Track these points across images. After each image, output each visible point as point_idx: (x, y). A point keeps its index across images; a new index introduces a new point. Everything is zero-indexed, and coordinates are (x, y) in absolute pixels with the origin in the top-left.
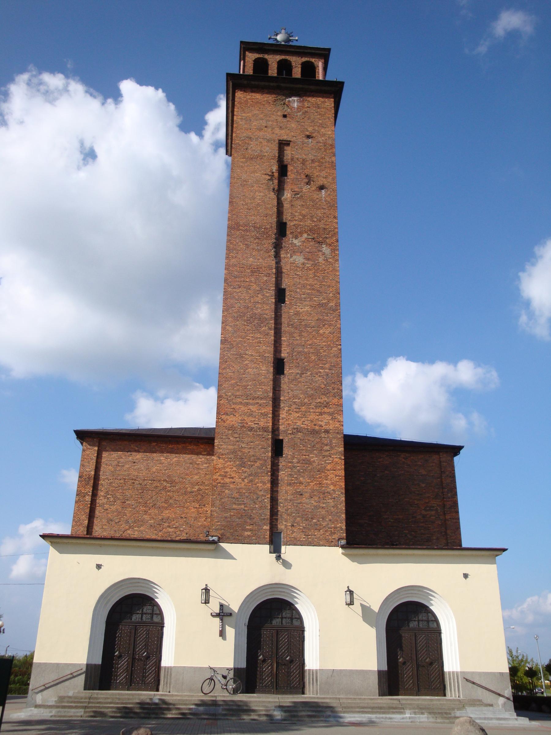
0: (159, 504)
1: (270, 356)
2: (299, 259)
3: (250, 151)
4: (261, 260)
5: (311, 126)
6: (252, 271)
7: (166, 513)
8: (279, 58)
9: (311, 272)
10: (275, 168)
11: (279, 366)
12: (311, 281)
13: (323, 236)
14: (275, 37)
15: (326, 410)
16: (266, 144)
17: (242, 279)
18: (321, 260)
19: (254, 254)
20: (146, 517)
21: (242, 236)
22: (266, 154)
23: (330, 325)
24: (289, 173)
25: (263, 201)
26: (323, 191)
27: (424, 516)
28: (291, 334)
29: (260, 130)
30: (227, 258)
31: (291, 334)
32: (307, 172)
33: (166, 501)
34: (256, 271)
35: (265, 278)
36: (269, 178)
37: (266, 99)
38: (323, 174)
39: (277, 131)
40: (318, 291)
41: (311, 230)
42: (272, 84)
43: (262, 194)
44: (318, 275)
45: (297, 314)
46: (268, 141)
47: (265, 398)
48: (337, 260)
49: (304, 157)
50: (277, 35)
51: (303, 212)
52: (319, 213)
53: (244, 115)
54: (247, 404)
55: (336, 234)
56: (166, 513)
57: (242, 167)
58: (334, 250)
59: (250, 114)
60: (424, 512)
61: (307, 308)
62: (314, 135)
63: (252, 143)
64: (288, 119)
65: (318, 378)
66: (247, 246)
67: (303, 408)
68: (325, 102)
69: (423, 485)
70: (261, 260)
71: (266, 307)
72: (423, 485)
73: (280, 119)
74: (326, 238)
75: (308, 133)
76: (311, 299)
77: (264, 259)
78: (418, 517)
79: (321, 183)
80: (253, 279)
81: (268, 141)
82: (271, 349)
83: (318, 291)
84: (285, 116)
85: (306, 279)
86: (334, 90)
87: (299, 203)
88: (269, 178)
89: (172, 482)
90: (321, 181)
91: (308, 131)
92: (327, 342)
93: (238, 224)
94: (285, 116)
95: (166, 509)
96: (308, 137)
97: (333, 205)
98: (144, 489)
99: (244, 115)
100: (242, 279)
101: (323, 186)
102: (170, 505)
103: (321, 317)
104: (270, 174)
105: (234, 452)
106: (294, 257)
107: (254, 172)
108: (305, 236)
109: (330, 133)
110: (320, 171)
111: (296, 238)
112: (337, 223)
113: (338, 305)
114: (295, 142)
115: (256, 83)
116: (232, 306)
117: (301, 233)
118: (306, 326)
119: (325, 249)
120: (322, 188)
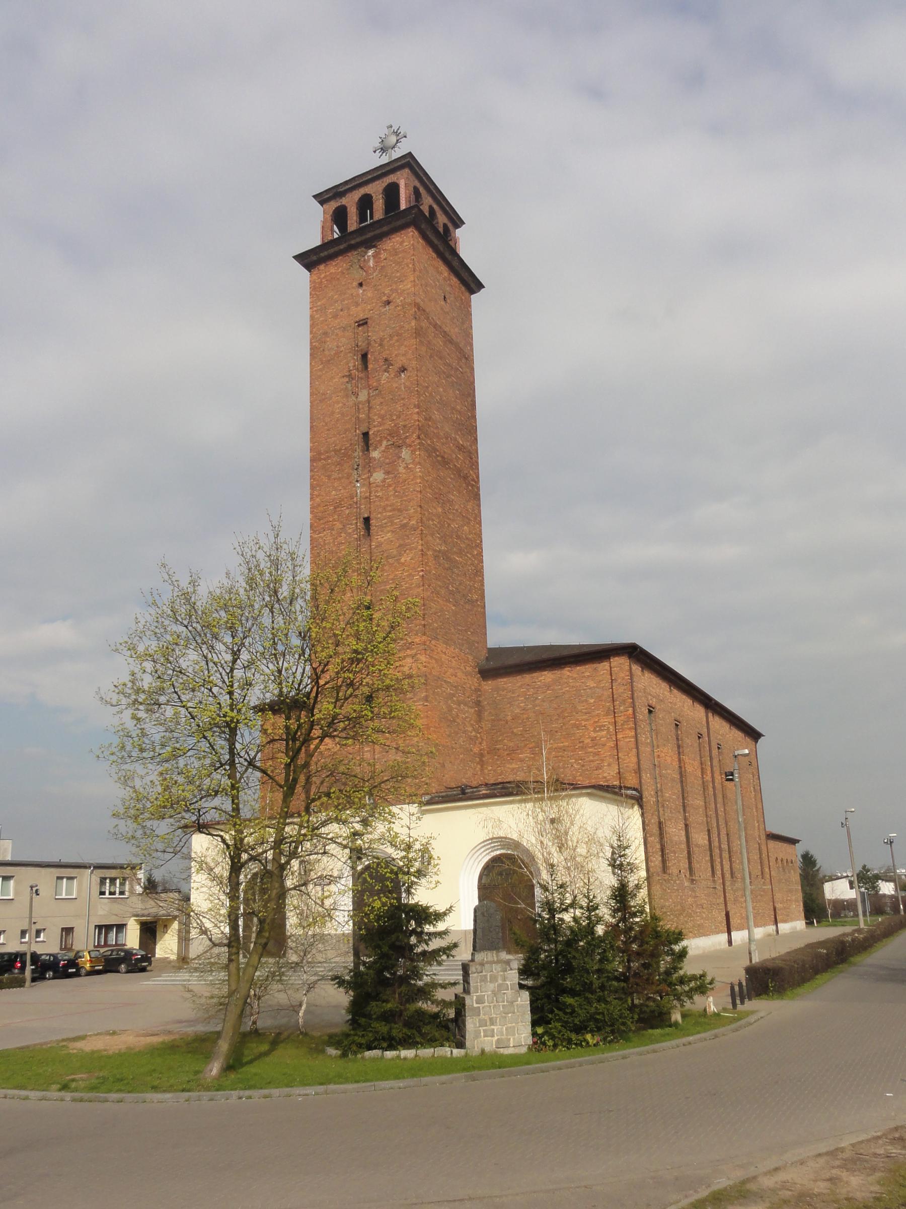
2: (378, 476)
3: (327, 352)
6: (335, 508)
8: (356, 195)
15: (409, 652)
17: (325, 520)
18: (401, 469)
23: (411, 550)
27: (593, 739)
29: (335, 316)
30: (312, 499)
36: (347, 380)
39: (354, 310)
40: (399, 510)
42: (342, 247)
44: (398, 489)
45: (379, 545)
51: (383, 412)
57: (320, 377)
60: (593, 734)
64: (364, 287)
66: (329, 477)
68: (401, 243)
69: (592, 701)
72: (592, 701)
74: (406, 437)
75: (385, 298)
76: (392, 522)
77: (345, 489)
78: (586, 741)
80: (336, 517)
84: (361, 285)
85: (387, 499)
88: (347, 380)
90: (400, 361)
91: (385, 294)
92: (408, 571)
93: (320, 454)
94: (361, 285)
100: (325, 520)
101: (403, 367)
103: (402, 542)
106: (374, 475)
108: (385, 443)
115: (326, 253)
117: (380, 442)
118: (387, 557)
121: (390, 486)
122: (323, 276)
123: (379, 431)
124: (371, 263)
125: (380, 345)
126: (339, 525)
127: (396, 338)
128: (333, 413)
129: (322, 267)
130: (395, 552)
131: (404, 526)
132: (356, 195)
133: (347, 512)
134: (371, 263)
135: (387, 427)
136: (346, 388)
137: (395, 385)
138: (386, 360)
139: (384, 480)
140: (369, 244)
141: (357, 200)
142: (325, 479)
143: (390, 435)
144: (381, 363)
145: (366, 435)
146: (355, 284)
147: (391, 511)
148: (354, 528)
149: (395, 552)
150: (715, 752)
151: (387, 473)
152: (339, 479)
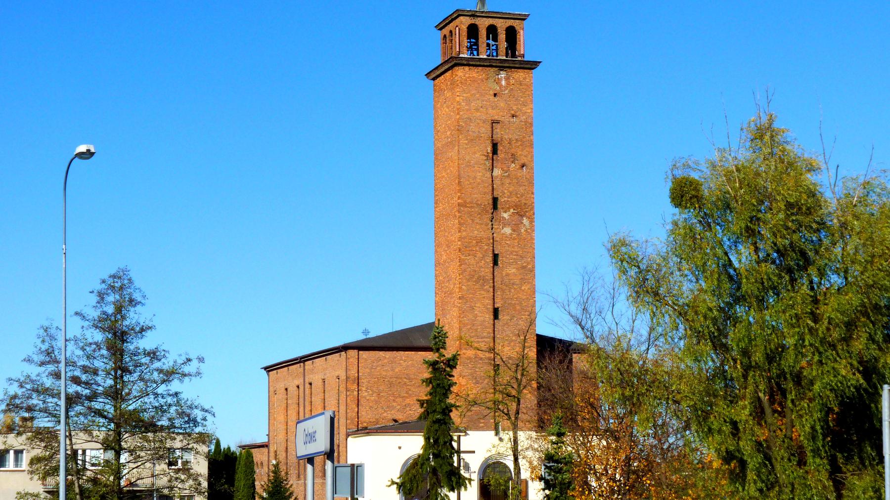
0: (402, 395)
1: (491, 307)
2: (508, 230)
7: (408, 401)
8: (488, 22)
10: (489, 149)
11: (496, 313)
13: (524, 210)
20: (395, 404)
21: (469, 213)
23: (529, 283)
24: (499, 152)
28: (503, 291)
29: (477, 110)
31: (503, 291)
32: (513, 151)
33: (407, 393)
34: (479, 241)
38: (525, 153)
39: (490, 111)
41: (516, 206)
45: (507, 275)
46: (484, 122)
47: (489, 337)
52: (522, 190)
54: (479, 342)
55: (533, 208)
56: (408, 401)
61: (514, 270)
65: (521, 322)
67: (512, 344)
71: (487, 270)
82: (491, 302)
84: (495, 95)
86: (532, 65)
87: (508, 181)
89: (410, 379)
90: (523, 160)
94: (495, 95)
95: (407, 397)
97: (531, 183)
98: (391, 384)
102: (410, 396)
105: (471, 374)
107: (475, 153)
108: (512, 210)
110: (522, 150)
113: (534, 267)
114: (503, 122)
116: (465, 271)
117: (509, 208)
119: (525, 221)
121: (515, 239)
124: (503, 83)
126: (479, 255)
128: (475, 178)
129: (467, 68)
130: (518, 282)
131: (524, 267)
132: (488, 22)
134: (503, 83)
135: (513, 199)
136: (485, 164)
139: (511, 234)
140: (502, 68)
145: (495, 200)
146: (492, 93)
148: (489, 259)
149: (518, 282)
150: (307, 386)
151: (514, 231)
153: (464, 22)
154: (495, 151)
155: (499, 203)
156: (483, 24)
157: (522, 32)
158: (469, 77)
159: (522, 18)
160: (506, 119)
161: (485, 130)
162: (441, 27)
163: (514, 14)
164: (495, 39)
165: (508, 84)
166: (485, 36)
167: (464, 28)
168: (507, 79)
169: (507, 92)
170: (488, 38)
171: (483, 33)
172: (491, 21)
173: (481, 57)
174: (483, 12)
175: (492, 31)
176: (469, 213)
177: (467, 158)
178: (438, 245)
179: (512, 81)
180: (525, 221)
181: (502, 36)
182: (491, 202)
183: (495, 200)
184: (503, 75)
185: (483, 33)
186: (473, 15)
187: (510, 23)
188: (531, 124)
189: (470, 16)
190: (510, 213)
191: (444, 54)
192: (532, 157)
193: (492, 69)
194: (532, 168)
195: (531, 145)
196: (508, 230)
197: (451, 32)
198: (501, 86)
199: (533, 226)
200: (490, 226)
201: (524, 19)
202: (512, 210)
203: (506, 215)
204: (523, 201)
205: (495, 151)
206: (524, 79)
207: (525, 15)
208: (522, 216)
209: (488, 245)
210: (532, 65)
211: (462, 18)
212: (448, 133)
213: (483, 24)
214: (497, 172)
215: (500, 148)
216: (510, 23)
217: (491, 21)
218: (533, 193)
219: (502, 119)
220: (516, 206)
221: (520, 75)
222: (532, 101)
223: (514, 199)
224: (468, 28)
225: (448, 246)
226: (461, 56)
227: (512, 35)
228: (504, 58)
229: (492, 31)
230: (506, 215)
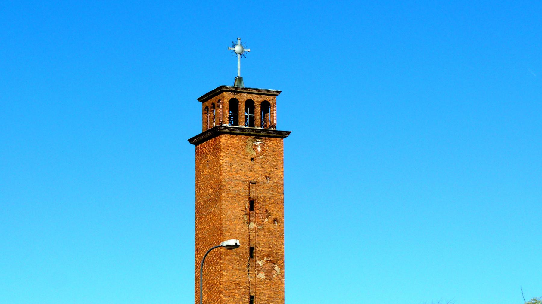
2: (262, 276)
4: (240, 278)
5: (269, 168)
6: (236, 286)
8: (247, 97)
9: (269, 285)
10: (247, 206)
12: (268, 292)
13: (276, 259)
14: (233, 49)
16: (241, 185)
17: (230, 291)
18: (274, 276)
19: (237, 272)
22: (241, 193)
24: (255, 208)
25: (241, 233)
26: (276, 222)
29: (237, 172)
32: (267, 207)
34: (238, 285)
35: (243, 290)
36: (244, 213)
37: (240, 144)
38: (277, 209)
39: (248, 173)
40: (273, 298)
41: (269, 255)
43: (240, 227)
44: (273, 287)
48: (284, 276)
49: (265, 195)
50: (234, 45)
51: (264, 240)
52: (274, 241)
53: (226, 159)
55: (283, 257)
57: (227, 205)
58: (282, 268)
59: (230, 159)
62: (270, 176)
63: (232, 184)
66: (233, 267)
70: (240, 278)
73: (249, 162)
74: (278, 260)
75: (267, 174)
79: (274, 217)
80: (236, 291)
81: (243, 182)
83: (273, 298)
86: (284, 134)
87: (262, 233)
88: (244, 213)
90: (275, 215)
96: (267, 177)
97: (281, 234)
99: (226, 159)
100: (230, 291)
104: (244, 210)
106: (259, 274)
107: (235, 209)
108: (265, 259)
109: (280, 174)
110: (274, 207)
111: (260, 260)
112: (284, 248)
117: (263, 257)
119: (277, 268)
120: (275, 220)
122: (229, 142)
123: (262, 250)
124: (259, 149)
125: (264, 201)
126: (238, 297)
127: (272, 200)
128: (235, 230)
129: (229, 136)
132: (247, 97)
133: (243, 290)
134: (259, 149)
136: (243, 218)
137: (272, 228)
138: (267, 211)
139: (265, 279)
140: (258, 137)
141: (245, 100)
142: (230, 268)
143: (269, 255)
144: (264, 211)
146: (249, 157)
147: (268, 297)
151: (267, 276)
152: (240, 270)
153: (227, 96)
154: (252, 207)
155: (254, 251)
156: (243, 98)
157: (275, 106)
158: (230, 144)
159: (275, 94)
160: (261, 180)
161: (243, 190)
162: (202, 100)
163: (268, 91)
164: (252, 111)
165: (263, 150)
166: (244, 108)
167: (226, 101)
168: (262, 146)
169: (262, 157)
170: (246, 111)
171: (242, 106)
172: (249, 96)
173: (240, 126)
174: (242, 89)
175: (250, 104)
176: (229, 260)
177: (229, 213)
178: (197, 288)
179: (266, 148)
180: (277, 268)
181: (258, 109)
182: (248, 251)
183: (252, 249)
184: (259, 142)
185: (242, 106)
186: (234, 91)
187: (265, 98)
188: (282, 185)
189: (231, 91)
190: (264, 261)
191: (205, 122)
192: (283, 212)
193: (249, 137)
194: (283, 223)
195: (282, 203)
196: (262, 276)
197: (213, 104)
198: (257, 152)
199: (283, 272)
200: (247, 272)
201: (276, 95)
202: (265, 259)
203: (260, 263)
204: (275, 251)
205: (252, 207)
206: (277, 146)
207: (277, 92)
208: (274, 263)
209: (245, 288)
210: (284, 134)
211: (224, 93)
212: (211, 191)
213: (243, 98)
214: (252, 225)
215: (256, 205)
216: (265, 98)
217: (249, 96)
218: (283, 244)
219: (258, 180)
220: (269, 255)
221: (273, 142)
222: (282, 165)
223: (267, 248)
224: (229, 102)
225: (209, 289)
226: (224, 125)
227: (266, 107)
228: (260, 128)
229: (250, 104)
230: (260, 263)
